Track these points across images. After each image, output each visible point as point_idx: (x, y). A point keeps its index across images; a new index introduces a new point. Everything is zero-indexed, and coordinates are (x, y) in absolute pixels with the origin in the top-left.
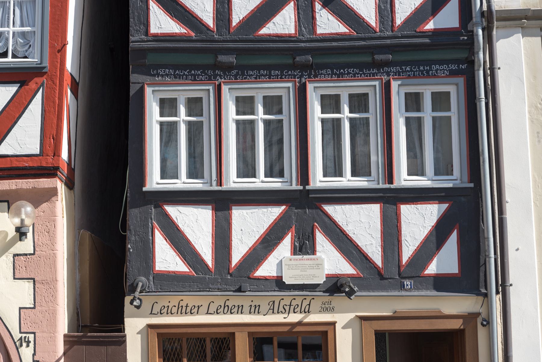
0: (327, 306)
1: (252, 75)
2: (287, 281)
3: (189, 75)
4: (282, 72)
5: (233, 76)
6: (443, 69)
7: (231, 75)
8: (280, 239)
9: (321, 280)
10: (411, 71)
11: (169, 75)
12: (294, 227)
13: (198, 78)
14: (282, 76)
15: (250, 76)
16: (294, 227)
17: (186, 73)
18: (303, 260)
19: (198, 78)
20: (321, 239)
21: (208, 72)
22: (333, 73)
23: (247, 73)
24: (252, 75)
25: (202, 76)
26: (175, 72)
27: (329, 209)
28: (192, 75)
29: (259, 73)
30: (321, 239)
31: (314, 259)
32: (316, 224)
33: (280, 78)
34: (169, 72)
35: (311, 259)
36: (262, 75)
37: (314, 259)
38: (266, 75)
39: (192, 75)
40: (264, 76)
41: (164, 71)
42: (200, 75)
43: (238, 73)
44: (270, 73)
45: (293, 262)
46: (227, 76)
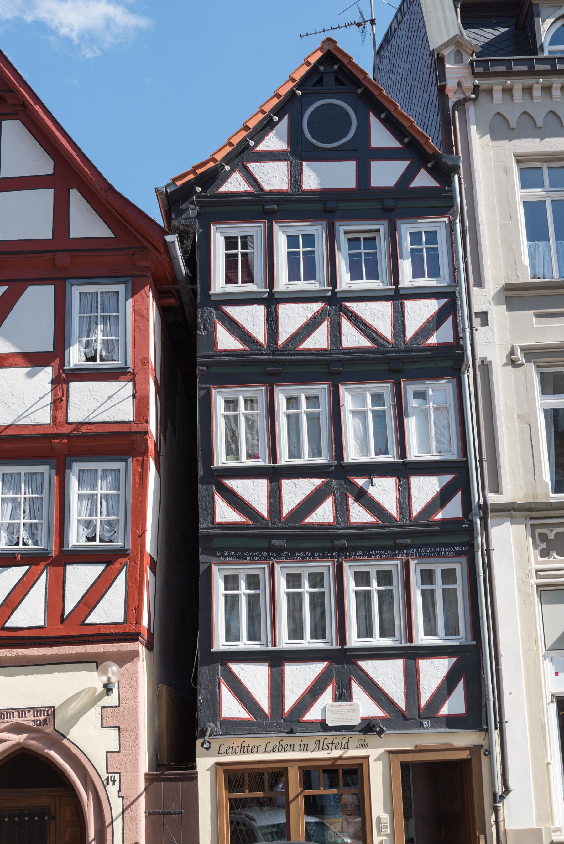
0: (362, 743)
1: (299, 556)
2: (330, 723)
3: (248, 556)
4: (323, 554)
5: (284, 557)
6: (450, 551)
7: (282, 556)
8: (324, 689)
10: (425, 552)
11: (231, 556)
12: (334, 679)
13: (255, 558)
14: (323, 557)
15: (298, 556)
17: (246, 554)
18: (342, 706)
19: (255, 558)
20: (356, 689)
21: (263, 553)
22: (364, 555)
23: (295, 554)
24: (299, 556)
25: (259, 557)
26: (236, 554)
27: (363, 664)
28: (250, 556)
29: (305, 554)
30: (356, 689)
31: (351, 705)
32: (352, 676)
33: (323, 558)
34: (232, 554)
35: (349, 705)
36: (308, 556)
37: (351, 705)
38: (311, 556)
39: (250, 556)
40: (309, 556)
41: (228, 553)
42: (257, 556)
43: (288, 554)
44: (314, 554)
45: (334, 708)
46: (279, 556)
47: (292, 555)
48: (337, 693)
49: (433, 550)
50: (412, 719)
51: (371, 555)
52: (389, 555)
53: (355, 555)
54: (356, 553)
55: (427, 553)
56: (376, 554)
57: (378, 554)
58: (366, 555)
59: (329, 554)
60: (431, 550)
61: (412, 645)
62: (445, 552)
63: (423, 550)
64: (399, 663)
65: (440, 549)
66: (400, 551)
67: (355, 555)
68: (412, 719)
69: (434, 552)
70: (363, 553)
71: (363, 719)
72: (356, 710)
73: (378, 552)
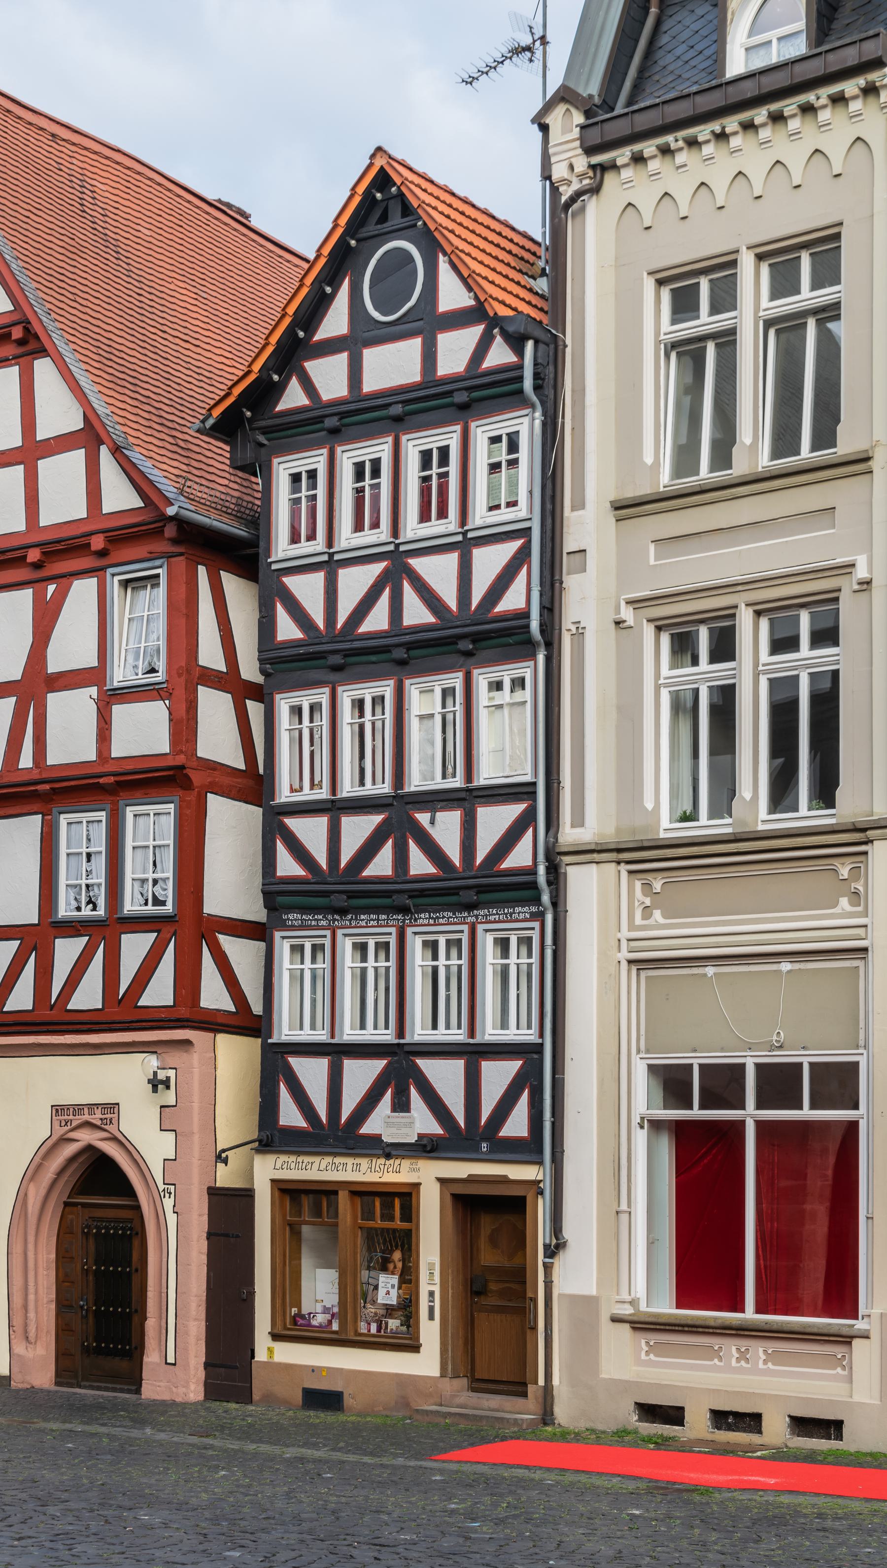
1: (363, 920)
4: (388, 917)
6: (525, 912)
8: (381, 1095)
9: (413, 1139)
10: (497, 914)
12: (393, 1082)
14: (388, 920)
16: (393, 1082)
20: (415, 1096)
22: (430, 918)
24: (363, 920)
30: (415, 1096)
32: (411, 1080)
33: (387, 923)
38: (375, 920)
44: (378, 917)
45: (391, 1120)
47: (356, 919)
48: (396, 1101)
49: (506, 911)
50: (471, 1139)
51: (438, 918)
52: (457, 918)
53: (421, 918)
54: (422, 915)
55: (499, 915)
56: (444, 917)
57: (445, 917)
58: (432, 918)
59: (394, 917)
60: (504, 911)
61: (471, 1041)
62: (519, 913)
63: (494, 912)
64: (459, 1065)
65: (514, 910)
66: (469, 913)
67: (421, 918)
68: (471, 1139)
69: (506, 914)
70: (430, 915)
71: (421, 1136)
72: (411, 1124)
73: (445, 914)
